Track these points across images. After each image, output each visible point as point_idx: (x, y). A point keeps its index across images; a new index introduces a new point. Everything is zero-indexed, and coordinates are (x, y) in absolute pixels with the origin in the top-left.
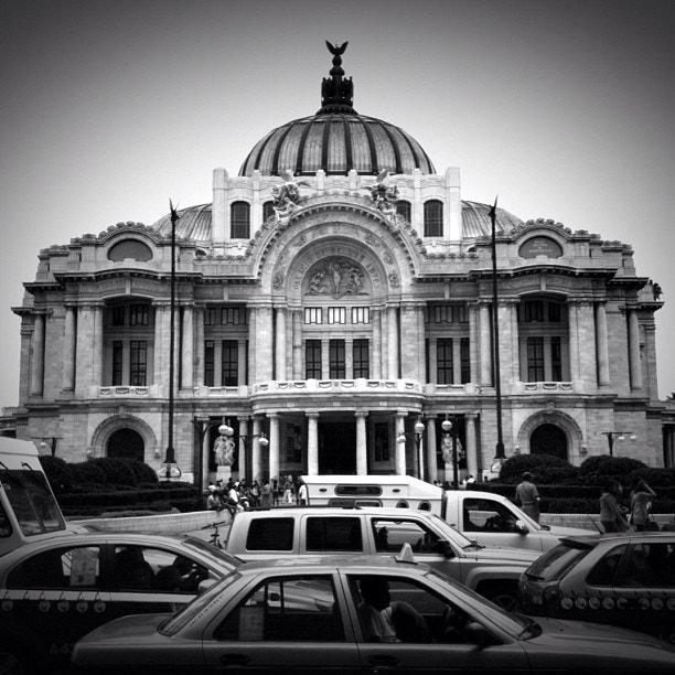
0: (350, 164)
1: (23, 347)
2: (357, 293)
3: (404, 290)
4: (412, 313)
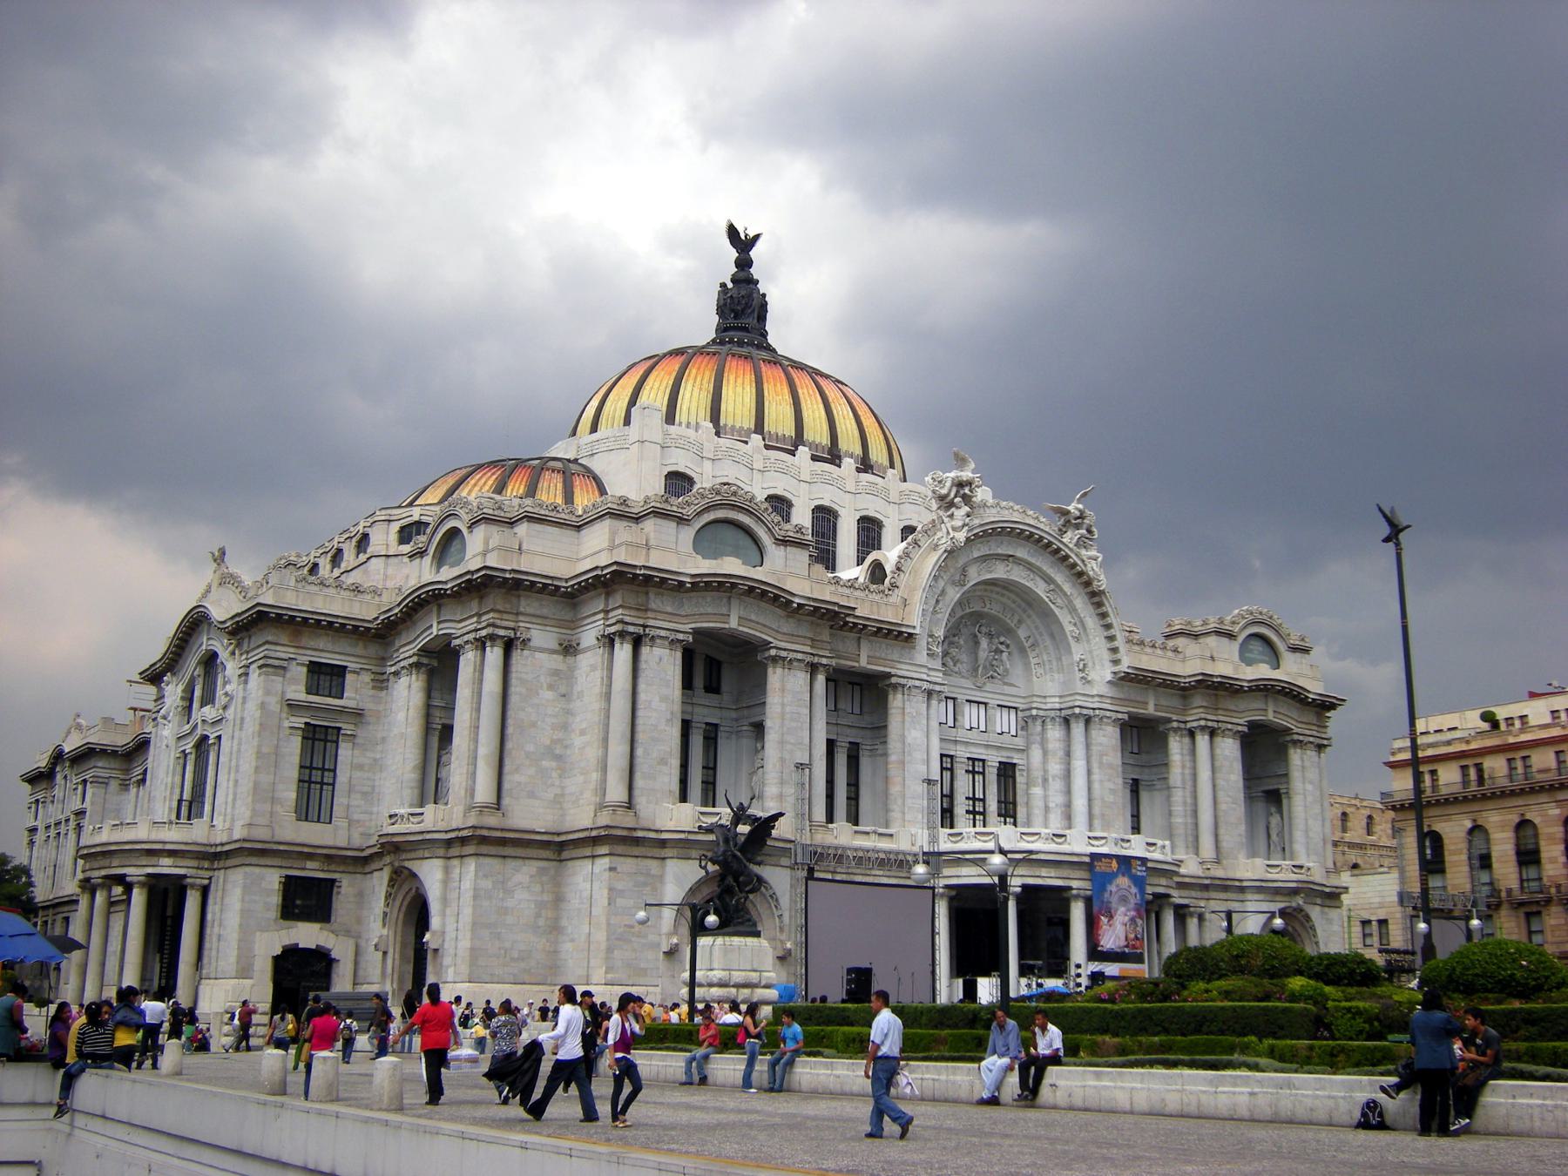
1: (267, 692)
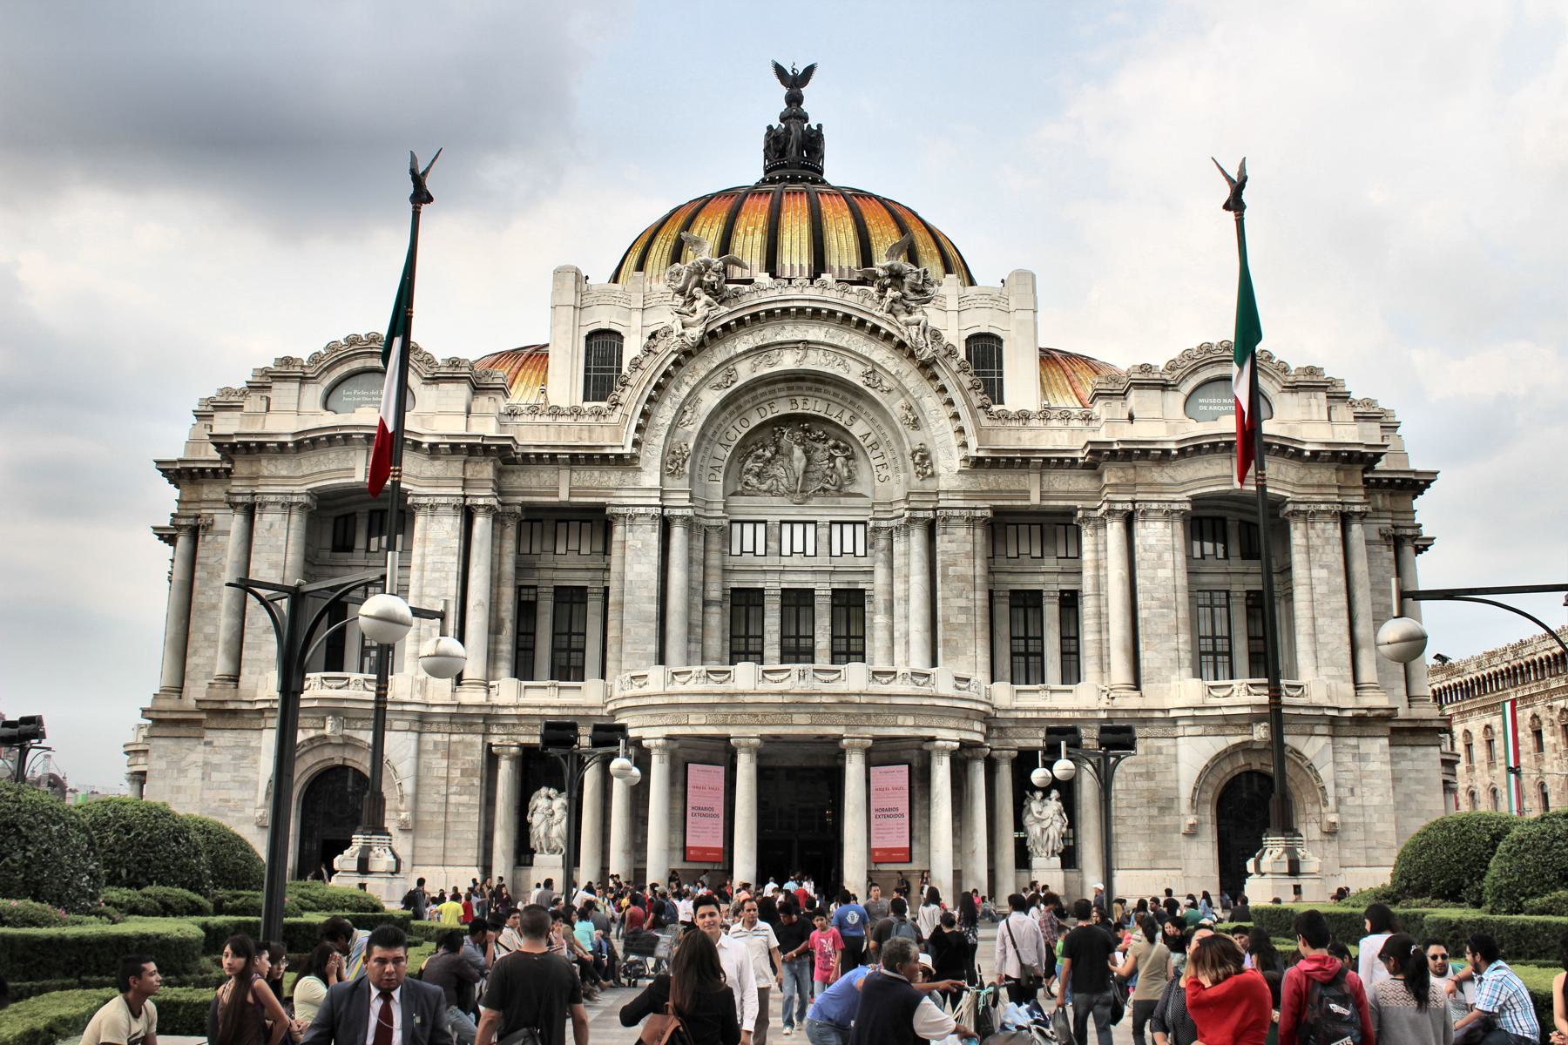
0: (819, 265)
2: (840, 491)
3: (943, 484)
4: (961, 532)
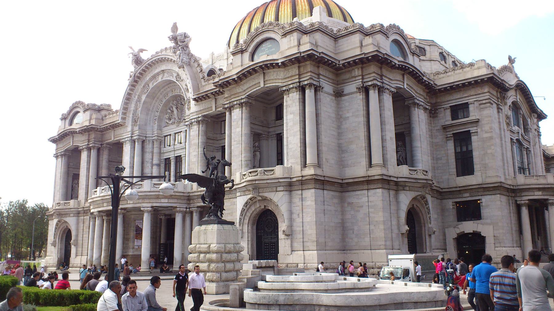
4: (195, 128)
